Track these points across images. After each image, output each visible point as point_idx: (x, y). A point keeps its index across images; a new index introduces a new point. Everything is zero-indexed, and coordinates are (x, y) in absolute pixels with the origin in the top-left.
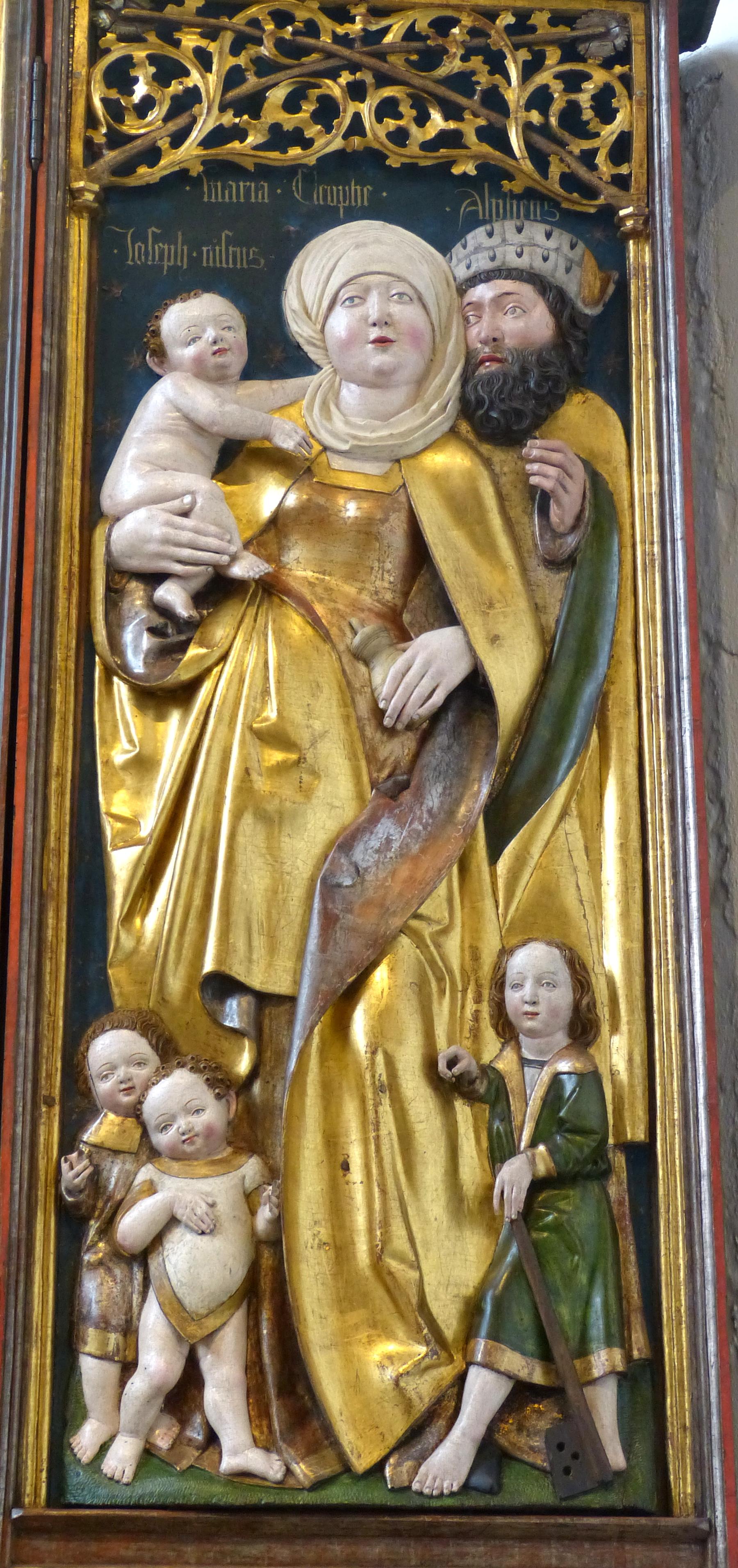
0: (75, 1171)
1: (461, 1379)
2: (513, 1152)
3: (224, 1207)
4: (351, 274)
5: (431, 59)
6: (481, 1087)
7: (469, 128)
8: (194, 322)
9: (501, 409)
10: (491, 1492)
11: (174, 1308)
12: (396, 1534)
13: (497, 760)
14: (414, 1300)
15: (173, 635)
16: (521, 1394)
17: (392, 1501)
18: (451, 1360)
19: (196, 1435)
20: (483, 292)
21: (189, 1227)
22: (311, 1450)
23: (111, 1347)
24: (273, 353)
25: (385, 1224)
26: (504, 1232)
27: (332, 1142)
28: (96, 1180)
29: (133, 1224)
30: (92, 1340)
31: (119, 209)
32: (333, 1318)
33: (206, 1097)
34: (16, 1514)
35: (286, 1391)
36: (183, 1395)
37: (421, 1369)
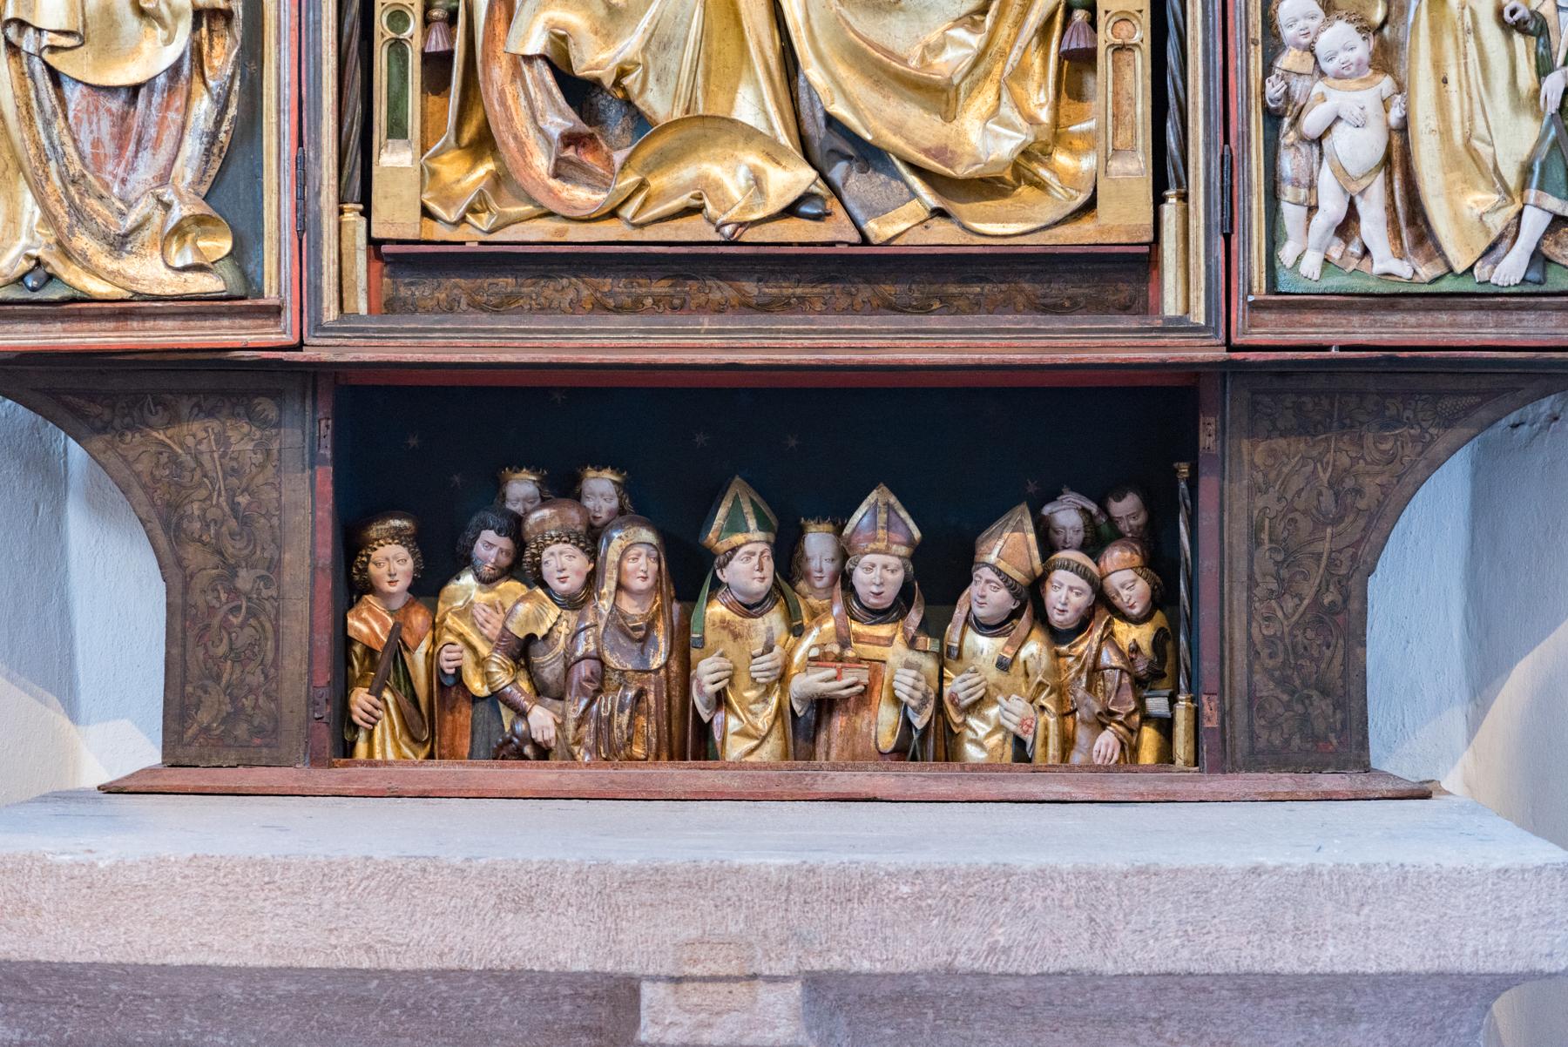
0: (1274, 89)
1: (1520, 213)
2: (1551, 69)
3: (1370, 110)
6: (1531, 27)
10: (1539, 283)
11: (1340, 172)
12: (1481, 308)
14: (1491, 166)
17: (1480, 289)
18: (1513, 202)
19: (1355, 249)
22: (1429, 259)
23: (1302, 198)
25: (1471, 119)
26: (1546, 120)
27: (1437, 65)
28: (1287, 94)
29: (1312, 122)
30: (1288, 192)
32: (1440, 176)
33: (1358, 37)
34: (1251, 299)
35: (1412, 221)
36: (1347, 226)
37: (1496, 209)
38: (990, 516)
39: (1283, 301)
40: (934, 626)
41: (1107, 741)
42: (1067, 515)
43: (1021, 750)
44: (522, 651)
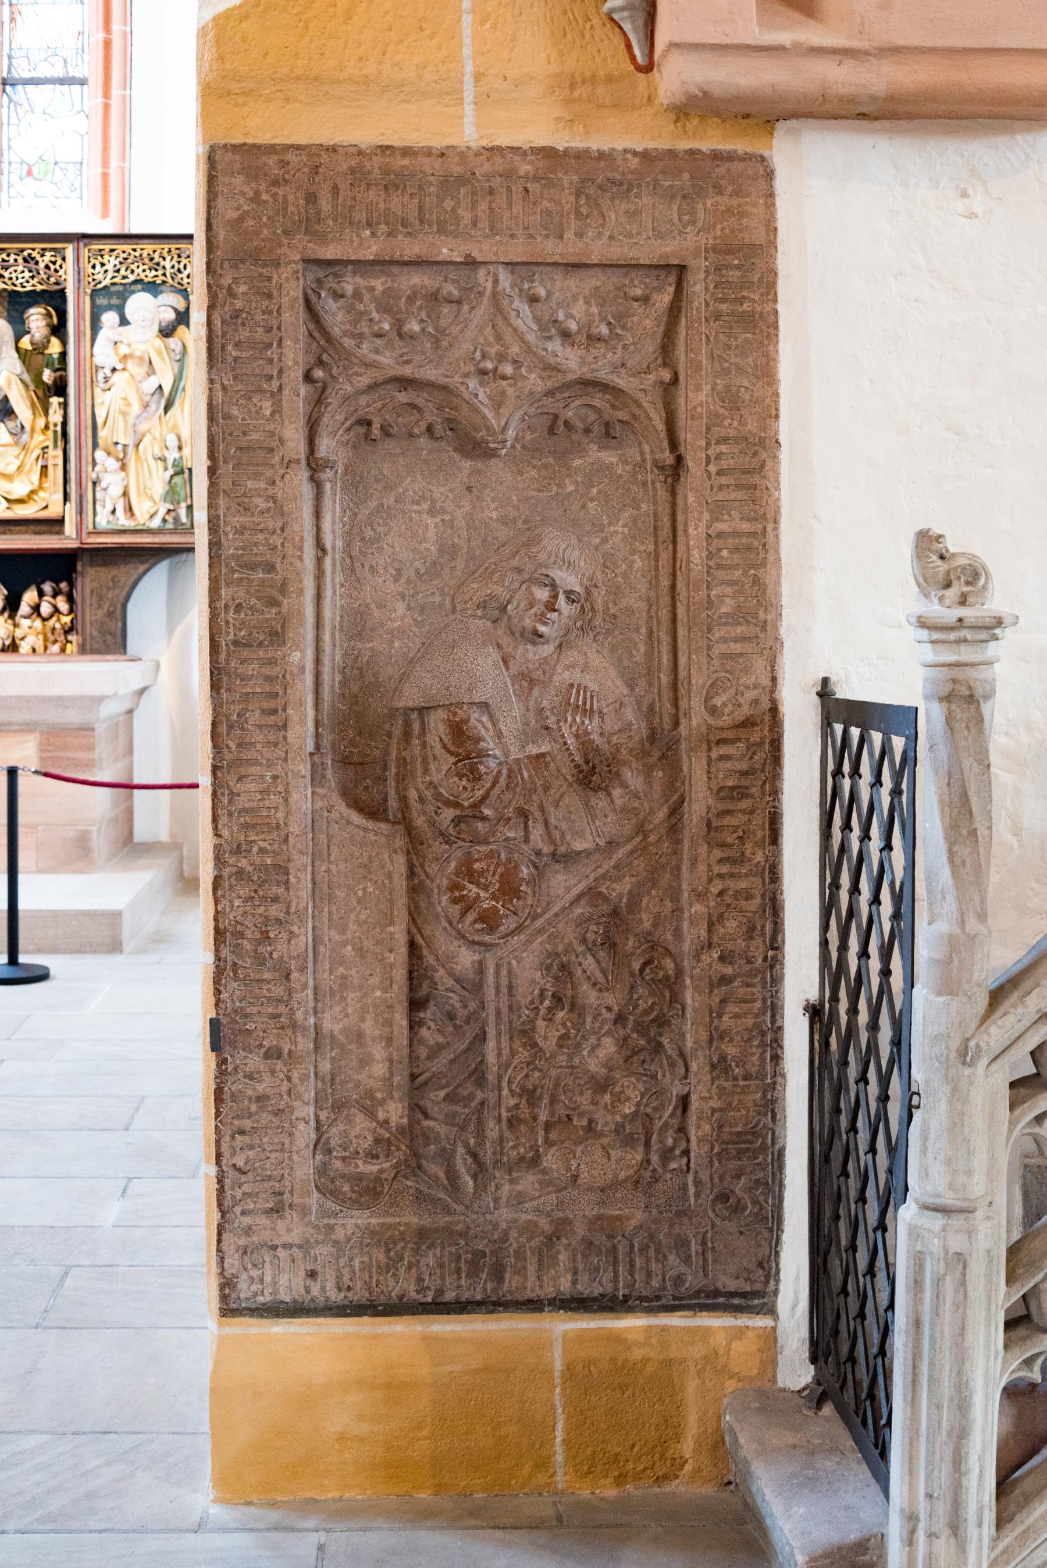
5: (152, 259)
7: (160, 272)
8: (109, 318)
15: (106, 379)
16: (169, 511)
20: (162, 308)
24: (124, 322)
29: (104, 484)
31: (95, 293)
38: (26, 588)
40: (12, 617)
41: (56, 648)
42: (47, 587)
43: (34, 650)
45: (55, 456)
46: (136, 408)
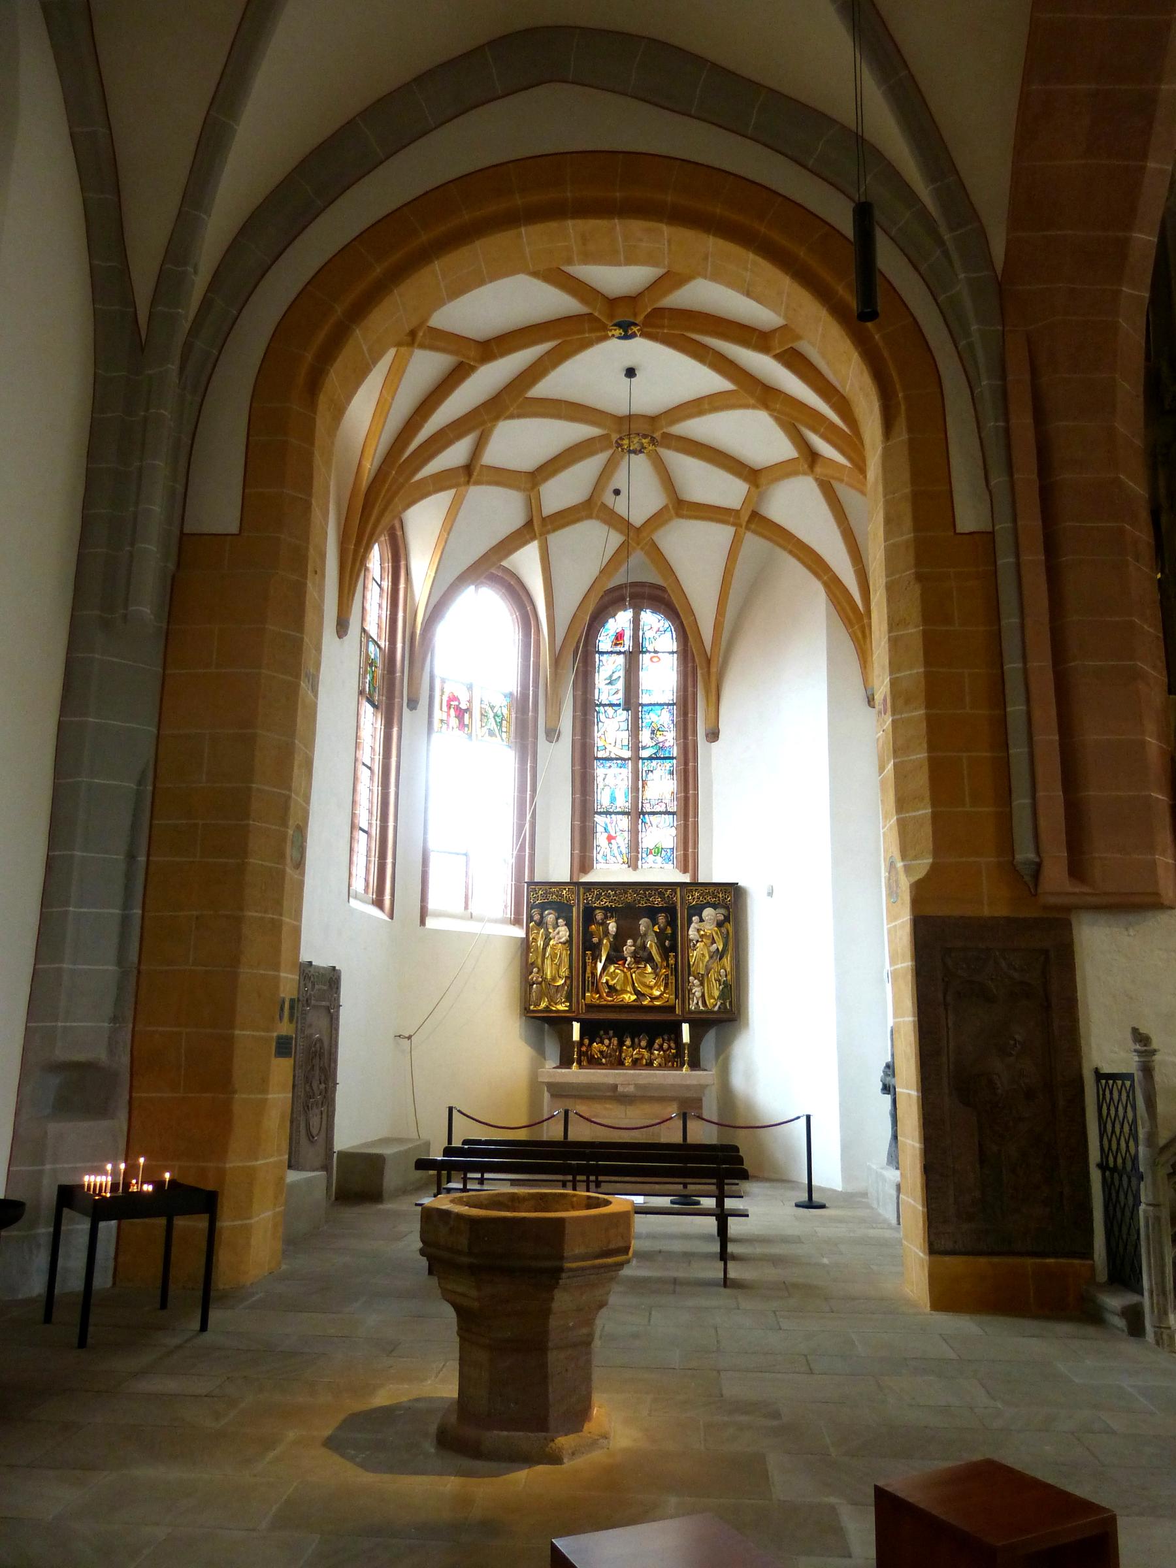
4: (708, 913)
9: (720, 925)
13: (721, 955)
21: (697, 991)
24: (702, 920)
39: (690, 1012)
44: (601, 1052)
45: (672, 979)
46: (707, 958)
